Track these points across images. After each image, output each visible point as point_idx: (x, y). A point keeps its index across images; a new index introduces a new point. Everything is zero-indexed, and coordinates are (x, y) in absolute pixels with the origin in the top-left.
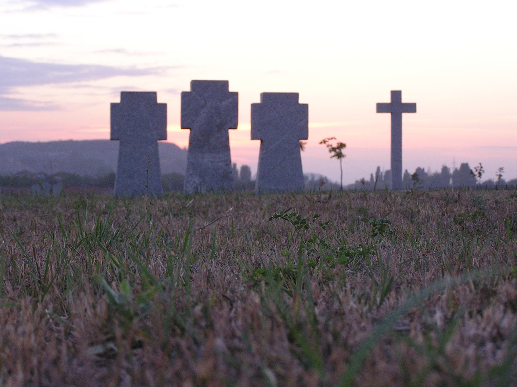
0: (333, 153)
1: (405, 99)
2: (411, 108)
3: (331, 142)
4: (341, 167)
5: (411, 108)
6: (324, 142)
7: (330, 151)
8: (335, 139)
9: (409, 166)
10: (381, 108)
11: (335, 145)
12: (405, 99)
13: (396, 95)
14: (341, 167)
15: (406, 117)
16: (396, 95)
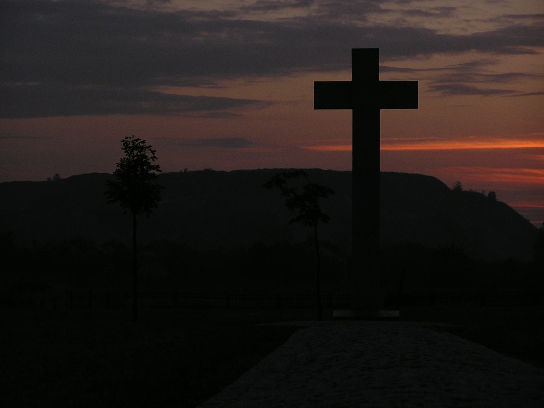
2: (405, 95)
5: (405, 95)
10: (326, 96)
13: (365, 61)
16: (365, 61)
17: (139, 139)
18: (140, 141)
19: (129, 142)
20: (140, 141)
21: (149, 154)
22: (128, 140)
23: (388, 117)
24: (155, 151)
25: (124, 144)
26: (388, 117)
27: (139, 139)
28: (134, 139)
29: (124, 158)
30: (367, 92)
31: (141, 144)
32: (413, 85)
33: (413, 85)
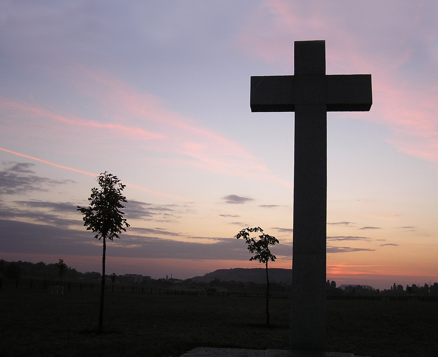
0: (255, 253)
1: (334, 66)
2: (355, 94)
3: (252, 235)
4: (267, 274)
6: (244, 234)
7: (251, 249)
8: (261, 230)
9: (339, 266)
10: (266, 95)
11: (258, 239)
12: (334, 66)
13: (310, 54)
14: (267, 274)
15: (339, 124)
16: (310, 54)
17: (110, 175)
18: (112, 176)
19: (103, 177)
20: (111, 177)
21: (116, 187)
22: (102, 175)
23: (335, 120)
24: (125, 186)
25: (100, 178)
26: (335, 120)
27: (110, 175)
28: (106, 174)
29: (94, 188)
30: (310, 94)
31: (113, 179)
32: (365, 81)
33: (365, 81)
